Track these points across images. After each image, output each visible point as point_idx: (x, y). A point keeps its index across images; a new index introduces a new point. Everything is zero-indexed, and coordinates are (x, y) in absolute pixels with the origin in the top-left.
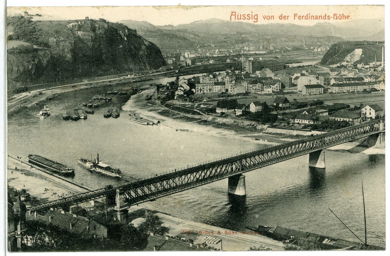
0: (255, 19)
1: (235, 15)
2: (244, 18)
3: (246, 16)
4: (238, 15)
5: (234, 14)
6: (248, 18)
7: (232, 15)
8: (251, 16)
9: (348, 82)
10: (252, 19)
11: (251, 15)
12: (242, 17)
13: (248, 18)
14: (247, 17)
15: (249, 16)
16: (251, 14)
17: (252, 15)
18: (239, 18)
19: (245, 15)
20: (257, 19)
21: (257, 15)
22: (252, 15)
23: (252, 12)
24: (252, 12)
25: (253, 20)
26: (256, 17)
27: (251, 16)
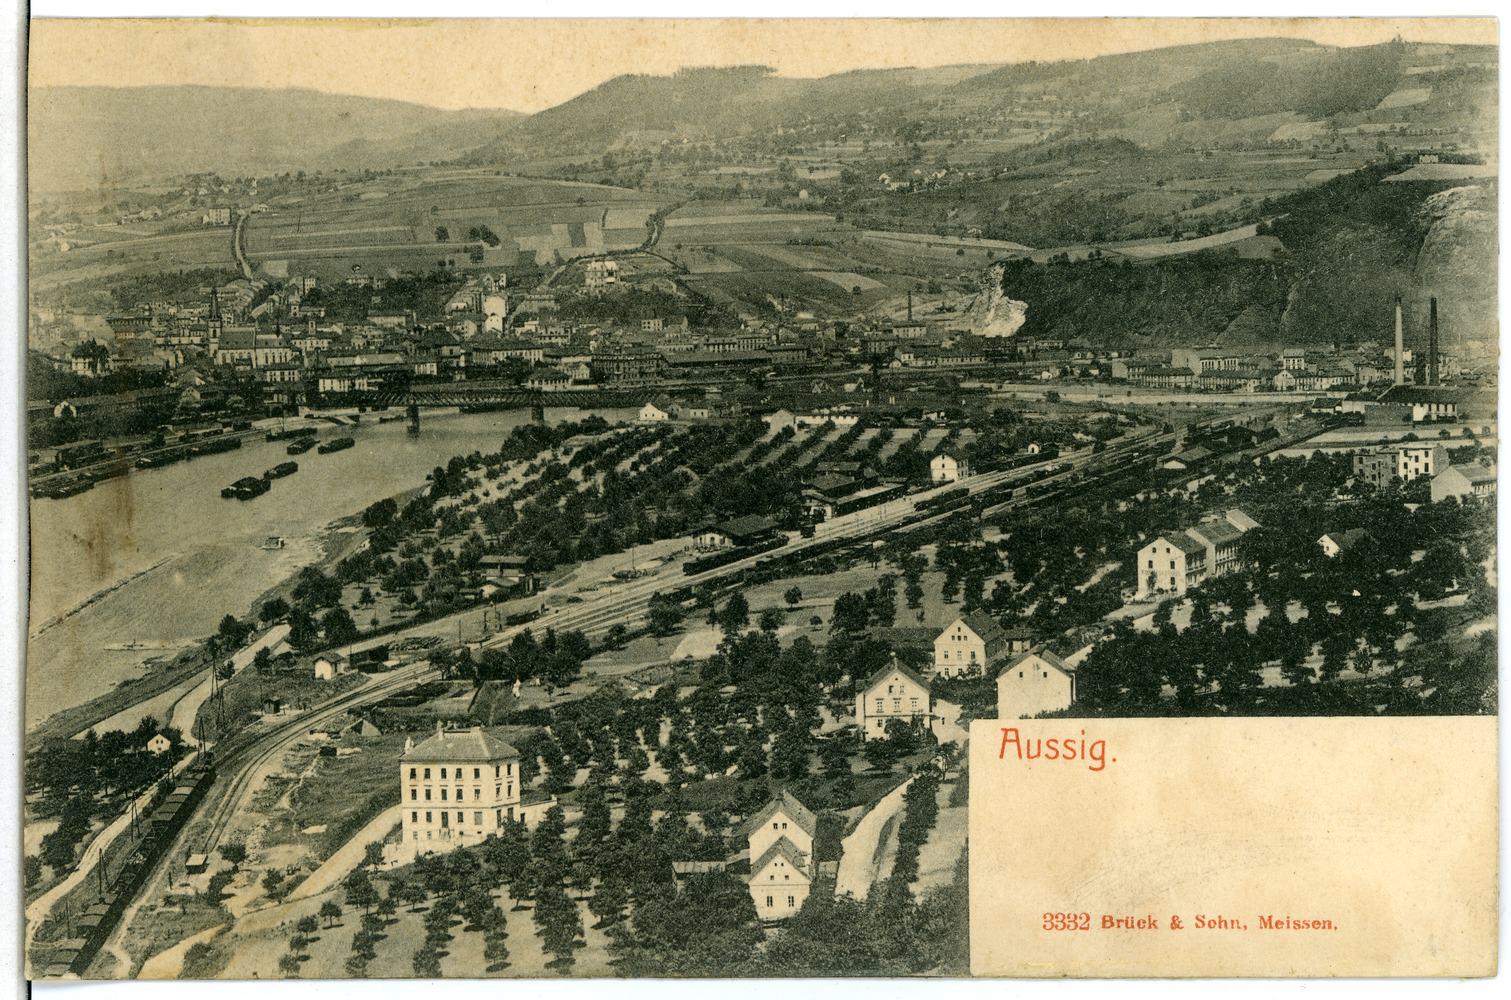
1: (1017, 740)
2: (1052, 753)
3: (1060, 747)
5: (1011, 735)
6: (1070, 754)
7: (1005, 740)
8: (1077, 747)
12: (1045, 749)
13: (1070, 754)
14: (1063, 750)
15: (1070, 744)
18: (1033, 752)
20: (1102, 758)
26: (1097, 752)
27: (1077, 747)
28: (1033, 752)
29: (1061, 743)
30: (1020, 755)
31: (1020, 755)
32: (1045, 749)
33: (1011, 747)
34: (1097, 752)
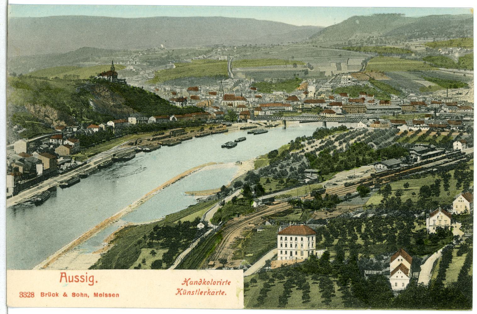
0: (90, 281)
1: (66, 276)
3: (79, 278)
4: (69, 277)
6: (82, 280)
7: (62, 276)
8: (85, 278)
9: (444, 247)
10: (87, 281)
11: (85, 277)
12: (74, 279)
13: (82, 280)
16: (85, 275)
17: (87, 276)
18: (71, 280)
19: (78, 276)
21: (93, 277)
22: (87, 276)
23: (87, 273)
24: (87, 273)
25: (89, 282)
26: (91, 279)
27: (85, 278)
28: (71, 280)
29: (80, 276)
30: (67, 281)
31: (67, 281)
32: (74, 279)
33: (64, 279)
34: (91, 279)
